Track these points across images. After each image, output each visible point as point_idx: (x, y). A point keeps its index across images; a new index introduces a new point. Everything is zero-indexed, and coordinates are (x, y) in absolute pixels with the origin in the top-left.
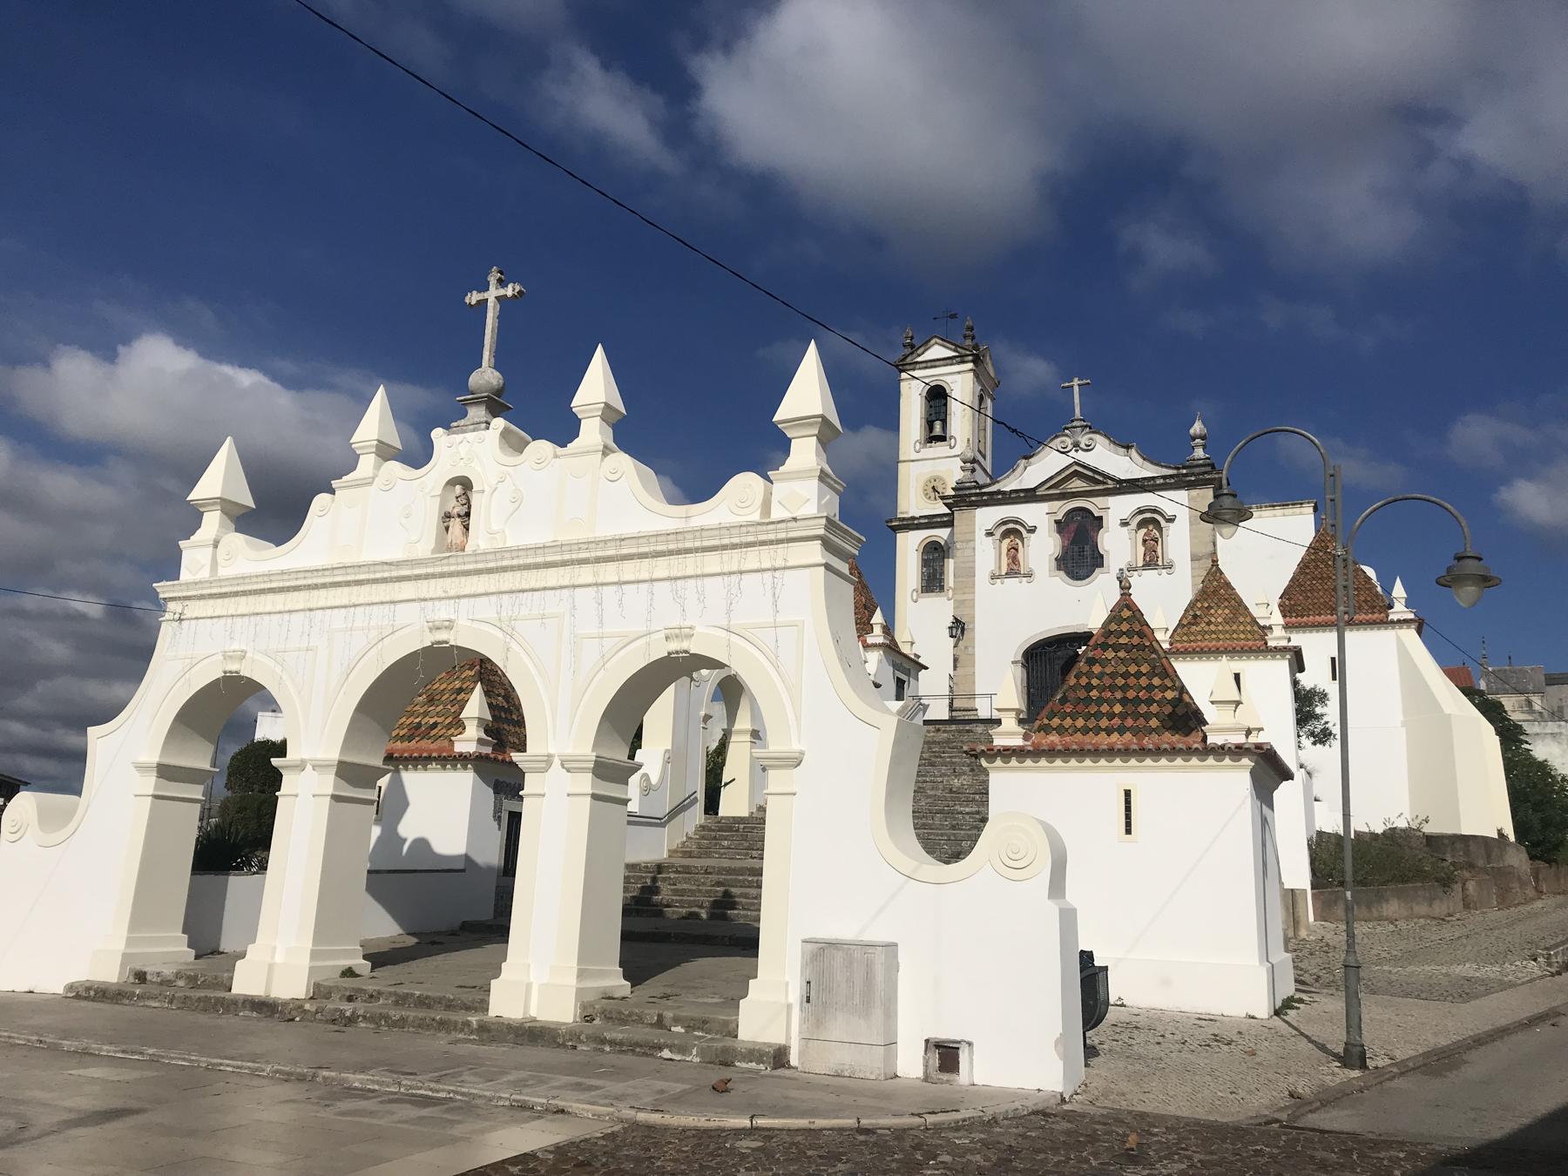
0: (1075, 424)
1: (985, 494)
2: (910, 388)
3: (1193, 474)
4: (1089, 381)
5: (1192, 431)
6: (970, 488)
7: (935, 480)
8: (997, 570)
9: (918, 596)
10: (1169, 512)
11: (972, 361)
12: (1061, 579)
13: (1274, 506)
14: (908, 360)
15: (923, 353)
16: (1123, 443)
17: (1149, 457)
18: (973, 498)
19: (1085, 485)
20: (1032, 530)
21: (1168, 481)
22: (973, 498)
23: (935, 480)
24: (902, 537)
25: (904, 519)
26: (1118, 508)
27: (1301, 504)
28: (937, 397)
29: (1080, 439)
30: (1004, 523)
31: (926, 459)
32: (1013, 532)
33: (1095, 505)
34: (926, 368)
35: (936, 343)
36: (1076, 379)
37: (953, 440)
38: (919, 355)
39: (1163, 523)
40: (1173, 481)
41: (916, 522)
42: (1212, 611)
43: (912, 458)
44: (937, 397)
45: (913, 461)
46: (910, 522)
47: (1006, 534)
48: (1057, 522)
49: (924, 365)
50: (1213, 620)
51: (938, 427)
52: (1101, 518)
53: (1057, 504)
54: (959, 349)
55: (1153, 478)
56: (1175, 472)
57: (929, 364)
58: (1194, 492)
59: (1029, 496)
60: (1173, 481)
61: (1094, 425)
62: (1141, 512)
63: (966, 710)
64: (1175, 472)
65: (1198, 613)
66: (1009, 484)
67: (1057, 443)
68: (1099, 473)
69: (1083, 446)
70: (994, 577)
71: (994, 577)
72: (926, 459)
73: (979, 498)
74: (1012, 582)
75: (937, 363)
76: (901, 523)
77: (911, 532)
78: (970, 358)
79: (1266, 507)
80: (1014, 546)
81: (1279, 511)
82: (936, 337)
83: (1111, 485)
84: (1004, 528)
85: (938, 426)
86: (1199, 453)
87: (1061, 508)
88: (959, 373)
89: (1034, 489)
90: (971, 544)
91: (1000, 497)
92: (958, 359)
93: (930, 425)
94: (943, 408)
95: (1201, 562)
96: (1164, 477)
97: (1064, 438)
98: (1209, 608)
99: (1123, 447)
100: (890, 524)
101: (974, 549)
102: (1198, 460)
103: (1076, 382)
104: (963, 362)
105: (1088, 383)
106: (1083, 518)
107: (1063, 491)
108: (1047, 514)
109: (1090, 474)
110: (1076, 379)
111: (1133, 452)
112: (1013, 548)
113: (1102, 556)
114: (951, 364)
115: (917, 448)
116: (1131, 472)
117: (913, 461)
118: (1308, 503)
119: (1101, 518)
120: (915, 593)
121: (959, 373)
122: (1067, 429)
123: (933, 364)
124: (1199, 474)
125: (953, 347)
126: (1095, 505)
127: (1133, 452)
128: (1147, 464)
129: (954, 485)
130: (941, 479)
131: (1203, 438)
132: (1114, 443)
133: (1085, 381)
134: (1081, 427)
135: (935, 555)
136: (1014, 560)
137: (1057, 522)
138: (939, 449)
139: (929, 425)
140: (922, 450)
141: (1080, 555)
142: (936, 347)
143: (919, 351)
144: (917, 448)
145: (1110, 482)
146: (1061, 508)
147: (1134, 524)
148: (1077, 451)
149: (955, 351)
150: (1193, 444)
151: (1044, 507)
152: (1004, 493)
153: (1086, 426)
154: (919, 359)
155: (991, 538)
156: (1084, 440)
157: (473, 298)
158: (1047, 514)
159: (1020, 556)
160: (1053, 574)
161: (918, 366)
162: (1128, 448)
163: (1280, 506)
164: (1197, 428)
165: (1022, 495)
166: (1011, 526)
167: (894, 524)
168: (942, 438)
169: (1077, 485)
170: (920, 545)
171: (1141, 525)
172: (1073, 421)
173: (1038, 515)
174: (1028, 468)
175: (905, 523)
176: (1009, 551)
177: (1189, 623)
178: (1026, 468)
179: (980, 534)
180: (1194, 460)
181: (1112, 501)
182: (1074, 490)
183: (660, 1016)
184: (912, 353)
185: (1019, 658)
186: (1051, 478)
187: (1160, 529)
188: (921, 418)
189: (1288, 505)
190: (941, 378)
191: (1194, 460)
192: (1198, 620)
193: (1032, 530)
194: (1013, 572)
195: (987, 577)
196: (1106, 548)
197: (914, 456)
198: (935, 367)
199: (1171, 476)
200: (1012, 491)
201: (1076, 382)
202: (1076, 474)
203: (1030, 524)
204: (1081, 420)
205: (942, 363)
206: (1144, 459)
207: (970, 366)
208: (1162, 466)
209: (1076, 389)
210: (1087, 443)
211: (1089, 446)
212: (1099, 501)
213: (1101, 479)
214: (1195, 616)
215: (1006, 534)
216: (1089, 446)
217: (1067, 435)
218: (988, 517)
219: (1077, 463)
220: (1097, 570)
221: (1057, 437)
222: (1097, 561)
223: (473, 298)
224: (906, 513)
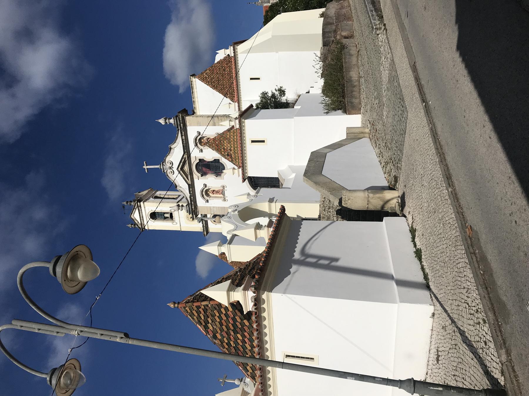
0: (162, 167)
1: (191, 203)
2: (151, 226)
3: (180, 125)
4: (144, 162)
5: (163, 124)
6: (189, 208)
7: (188, 217)
8: (222, 199)
10: (196, 134)
11: (140, 203)
13: (193, 92)
14: (140, 226)
15: (137, 221)
18: (193, 207)
19: (186, 165)
20: (205, 185)
21: (183, 134)
22: (193, 207)
23: (188, 217)
24: (211, 230)
25: (204, 230)
26: (196, 154)
27: (191, 81)
28: (154, 216)
29: (168, 167)
30: (203, 196)
31: (180, 220)
32: (206, 193)
33: (194, 162)
34: (143, 220)
35: (133, 216)
37: (172, 210)
38: (138, 222)
40: (183, 132)
41: (205, 225)
42: (225, 148)
43: (179, 226)
44: (154, 216)
45: (180, 225)
46: (205, 228)
47: (207, 195)
48: (202, 176)
49: (142, 221)
50: (229, 148)
51: (167, 215)
52: (200, 160)
53: (195, 176)
54: (135, 208)
55: (182, 140)
56: (180, 131)
57: (142, 219)
58: (188, 124)
59: (191, 187)
60: (183, 132)
61: (162, 161)
64: (180, 131)
65: (226, 154)
66: (188, 195)
67: (170, 175)
69: (171, 165)
70: (225, 200)
71: (225, 200)
72: (180, 220)
73: (193, 205)
75: (141, 216)
76: (205, 231)
77: (209, 227)
78: (139, 203)
79: (193, 95)
80: (212, 192)
81: (195, 90)
82: (131, 216)
83: (186, 156)
84: (205, 196)
85: (168, 215)
86: (172, 121)
87: (196, 174)
88: (145, 208)
89: (189, 185)
90: (212, 208)
91: (192, 197)
92: (139, 208)
93: (165, 218)
95: (216, 122)
96: (182, 136)
97: (168, 173)
98: (224, 149)
99: (170, 150)
100: (206, 235)
101: (214, 207)
102: (174, 122)
104: (140, 206)
106: (200, 166)
107: (189, 173)
108: (199, 179)
109: (181, 164)
111: (172, 146)
112: (213, 193)
113: (215, 160)
114: (141, 210)
116: (180, 147)
117: (180, 225)
118: (191, 79)
119: (200, 160)
121: (145, 208)
122: (164, 171)
123: (141, 217)
124: (180, 122)
125: (134, 210)
126: (194, 162)
127: (172, 146)
128: (177, 141)
129: (188, 214)
131: (166, 120)
132: (169, 153)
133: (145, 164)
134: (163, 166)
136: (217, 192)
137: (202, 176)
138: (175, 215)
139: (166, 218)
142: (134, 216)
143: (137, 222)
145: (184, 156)
146: (196, 174)
148: (173, 168)
149: (136, 209)
150: (168, 123)
153: (163, 164)
154: (140, 222)
155: (209, 201)
156: (169, 165)
158: (199, 179)
159: (216, 189)
160: (222, 178)
161: (143, 223)
162: (171, 149)
163: (192, 90)
164: (162, 121)
165: (191, 189)
166: (204, 193)
167: (205, 233)
168: (171, 214)
169: (186, 168)
172: (161, 169)
173: (199, 183)
174: (180, 186)
175: (205, 229)
177: (231, 158)
178: (180, 187)
179: (207, 205)
180: (175, 123)
181: (193, 156)
184: (137, 225)
186: (184, 178)
188: (163, 222)
189: (192, 87)
190: (147, 214)
191: (175, 123)
192: (229, 154)
193: (205, 185)
194: (223, 193)
195: (225, 202)
197: (179, 225)
198: (143, 216)
199: (181, 133)
200: (190, 193)
201: (145, 167)
202: (182, 169)
203: (203, 186)
204: (160, 166)
205: (141, 214)
206: (175, 142)
207: (142, 203)
208: (178, 136)
209: (148, 167)
210: (170, 164)
214: (228, 155)
215: (207, 195)
216: (170, 163)
217: (167, 171)
218: (200, 202)
221: (167, 175)
222: (217, 161)
224: (201, 228)
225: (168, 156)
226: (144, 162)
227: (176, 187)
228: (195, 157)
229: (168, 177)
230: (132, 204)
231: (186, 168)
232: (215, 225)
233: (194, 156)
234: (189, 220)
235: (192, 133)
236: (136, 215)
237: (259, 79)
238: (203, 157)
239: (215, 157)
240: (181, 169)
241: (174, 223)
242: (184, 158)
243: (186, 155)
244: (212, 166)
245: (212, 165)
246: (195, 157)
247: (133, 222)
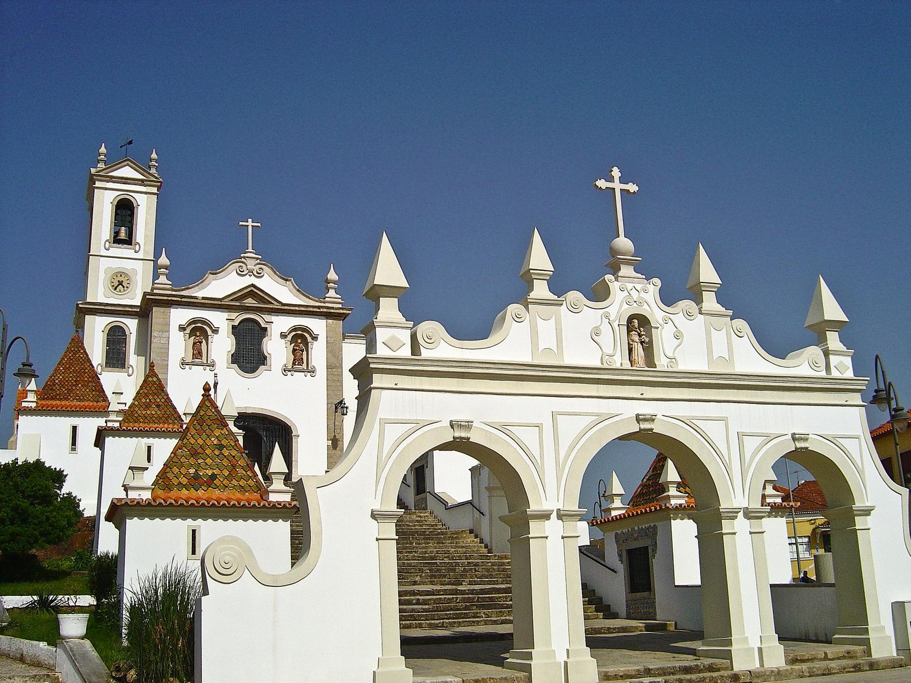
4: (259, 225)
16: (284, 275)
17: (302, 289)
20: (216, 331)
24: (88, 318)
26: (280, 324)
35: (128, 165)
36: (250, 220)
37: (137, 246)
39: (309, 339)
52: (265, 329)
53: (234, 315)
58: (330, 321)
62: (295, 329)
70: (184, 363)
71: (184, 363)
87: (238, 317)
88: (146, 193)
94: (129, 219)
103: (250, 223)
105: (259, 226)
108: (227, 319)
110: (250, 220)
113: (265, 358)
115: (107, 246)
119: (265, 329)
121: (146, 193)
130: (126, 275)
135: (116, 338)
137: (234, 327)
144: (107, 246)
146: (238, 317)
151: (225, 315)
157: (616, 173)
158: (227, 319)
168: (129, 241)
173: (220, 319)
181: (274, 318)
182: (247, 305)
183: (826, 654)
187: (306, 344)
193: (216, 331)
197: (104, 252)
201: (250, 223)
207: (155, 190)
211: (261, 273)
212: (267, 318)
213: (270, 300)
216: (261, 273)
218: (180, 316)
219: (253, 285)
223: (616, 173)
226: (259, 225)
228: (272, 323)
229: (237, 262)
230: (153, 171)
231: (249, 302)
232: (103, 330)
234: (115, 277)
235: (318, 326)
240: (253, 292)
241: (107, 243)
246: (272, 323)
247: (114, 162)
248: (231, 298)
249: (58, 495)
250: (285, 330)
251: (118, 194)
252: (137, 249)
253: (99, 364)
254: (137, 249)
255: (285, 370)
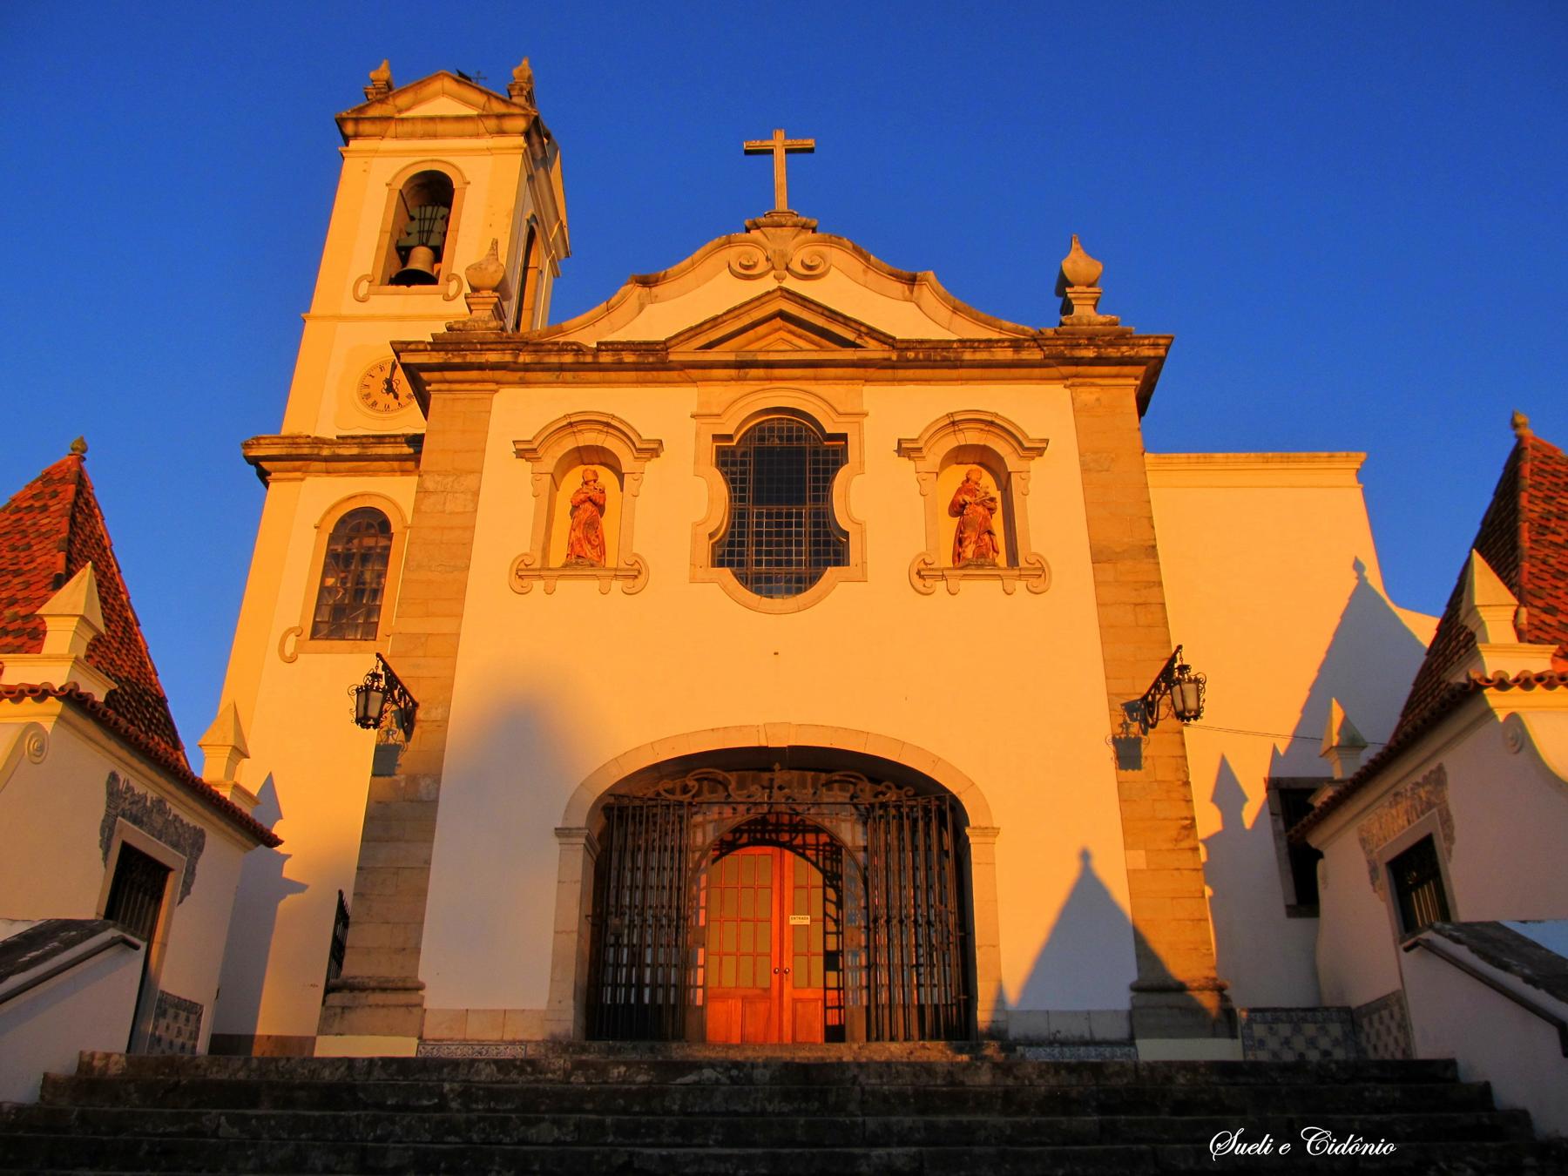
8: (538, 555)
9: (299, 648)
10: (1033, 431)
12: (724, 588)
20: (653, 450)
35: (444, 93)
39: (1012, 462)
62: (953, 424)
63: (384, 990)
68: (846, 321)
71: (524, 572)
74: (579, 591)
75: (440, 127)
83: (874, 351)
85: (420, 259)
89: (665, 345)
90: (469, 481)
93: (404, 252)
94: (438, 226)
99: (898, 277)
101: (476, 494)
104: (502, 132)
105: (811, 150)
112: (590, 499)
114: (477, 135)
120: (292, 638)
123: (431, 127)
127: (926, 294)
139: (401, 256)
140: (373, 298)
141: (779, 534)
147: (934, 457)
152: (579, 349)
156: (800, 249)
159: (608, 523)
162: (912, 281)
166: (590, 438)
168: (427, 279)
169: (781, 344)
170: (329, 512)
171: (959, 455)
174: (649, 308)
176: (576, 507)
178: (641, 308)
185: (580, 820)
186: (715, 321)
193: (653, 450)
196: (857, 514)
197: (349, 307)
198: (435, 136)
200: (603, 346)
201: (779, 142)
203: (648, 434)
207: (521, 140)
209: (780, 156)
210: (808, 262)
213: (850, 336)
216: (810, 268)
217: (756, 243)
220: (831, 572)
221: (729, 242)
225: (857, 265)
227: (646, 282)
233: (866, 408)
236: (444, 101)
237: (1292, 911)
238: (862, 463)
239: (863, 533)
242: (858, 341)
243: (886, 355)
244: (789, 515)
245: (799, 515)
248: (703, 340)
249: (461, 1104)
250: (912, 430)
251: (404, 165)
252: (452, 293)
253: (291, 631)
254: (452, 293)
255: (924, 573)
